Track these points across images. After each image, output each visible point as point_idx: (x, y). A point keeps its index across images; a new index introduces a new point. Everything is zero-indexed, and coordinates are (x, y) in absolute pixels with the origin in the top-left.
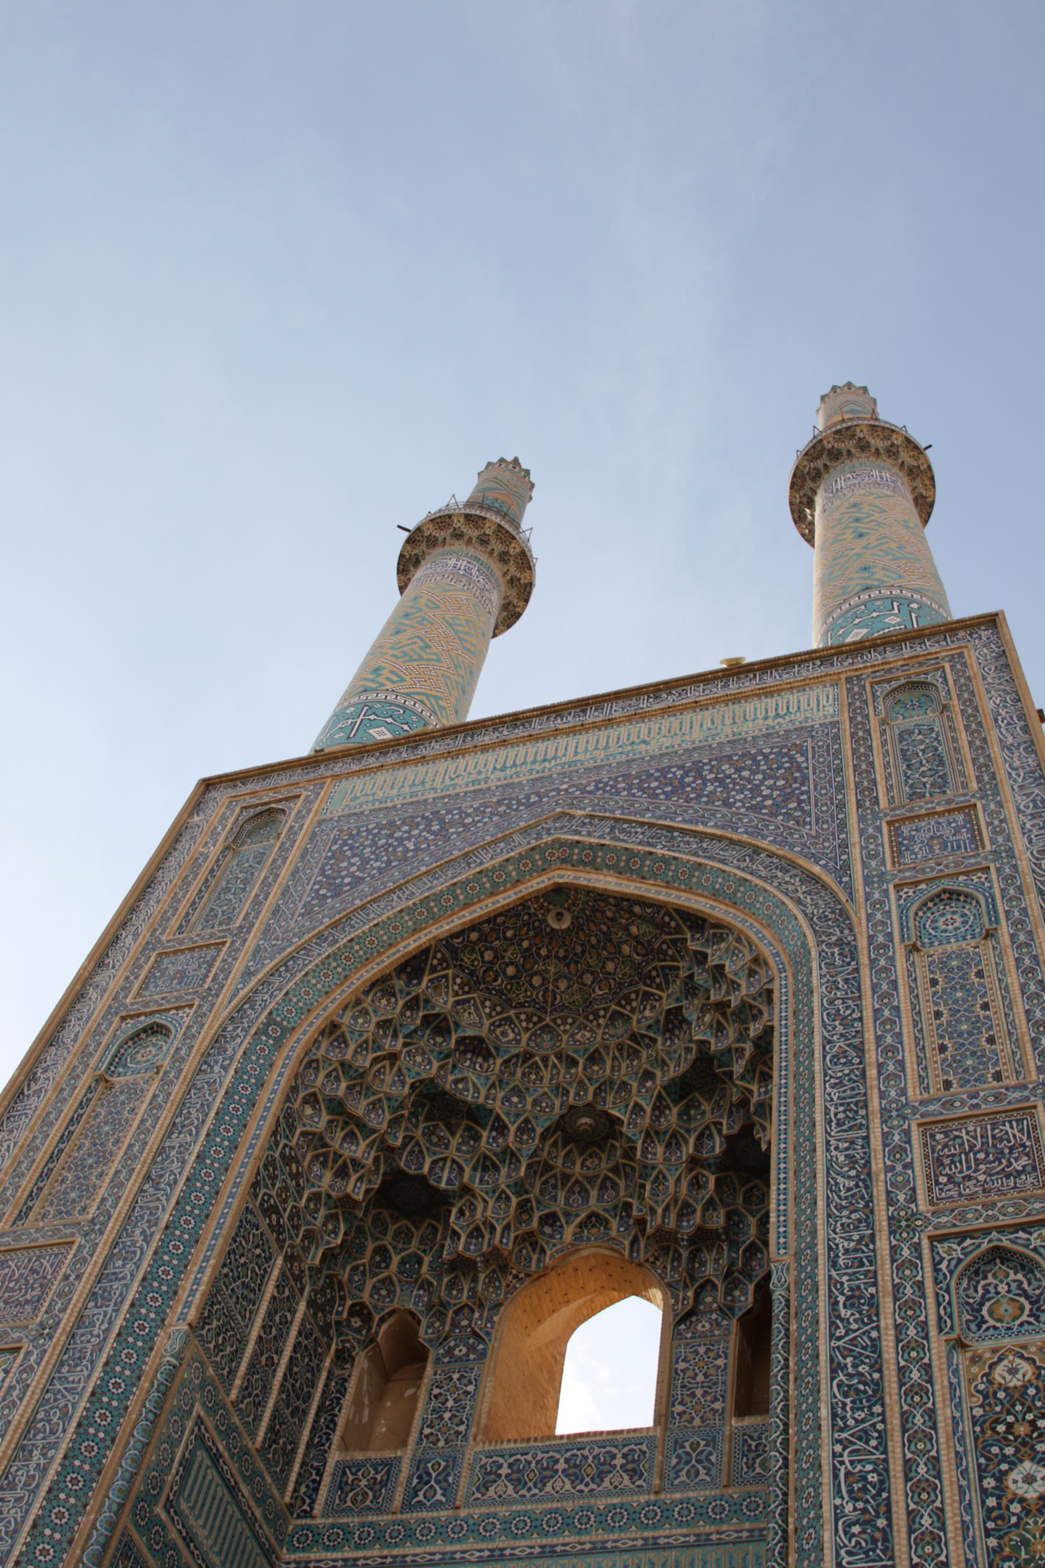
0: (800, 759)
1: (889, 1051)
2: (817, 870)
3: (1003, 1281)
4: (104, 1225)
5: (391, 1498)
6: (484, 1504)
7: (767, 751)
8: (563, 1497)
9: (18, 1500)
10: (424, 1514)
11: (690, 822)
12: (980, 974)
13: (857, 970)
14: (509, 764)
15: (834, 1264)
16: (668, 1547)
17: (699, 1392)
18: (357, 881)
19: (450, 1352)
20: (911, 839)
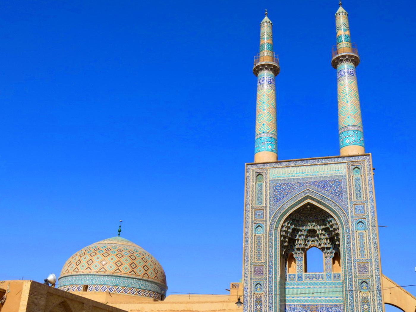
0: (341, 184)
1: (354, 250)
2: (345, 212)
3: (364, 284)
4: (267, 263)
5: (295, 279)
6: (307, 281)
7: (336, 180)
8: (315, 281)
9: (271, 300)
10: (300, 282)
11: (327, 196)
12: (364, 237)
13: (350, 234)
14: (297, 173)
15: (349, 280)
16: (327, 288)
17: (328, 268)
18: (280, 199)
19: (298, 259)
20: (356, 209)
